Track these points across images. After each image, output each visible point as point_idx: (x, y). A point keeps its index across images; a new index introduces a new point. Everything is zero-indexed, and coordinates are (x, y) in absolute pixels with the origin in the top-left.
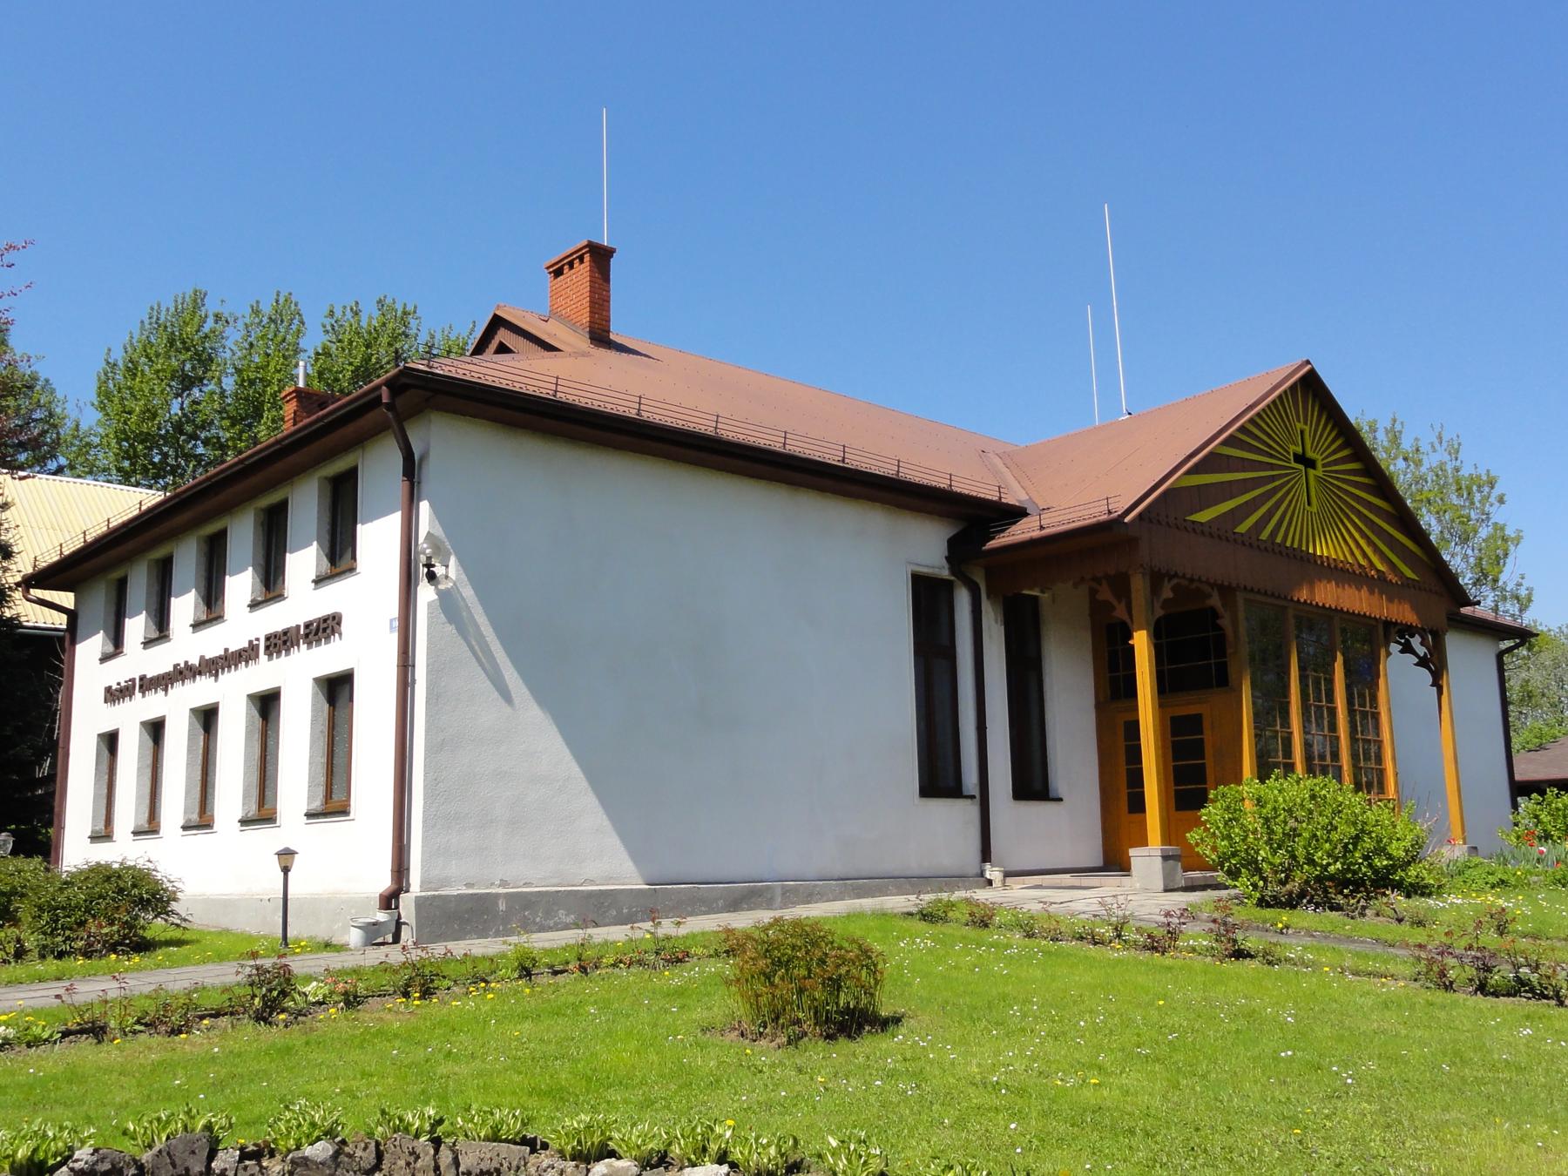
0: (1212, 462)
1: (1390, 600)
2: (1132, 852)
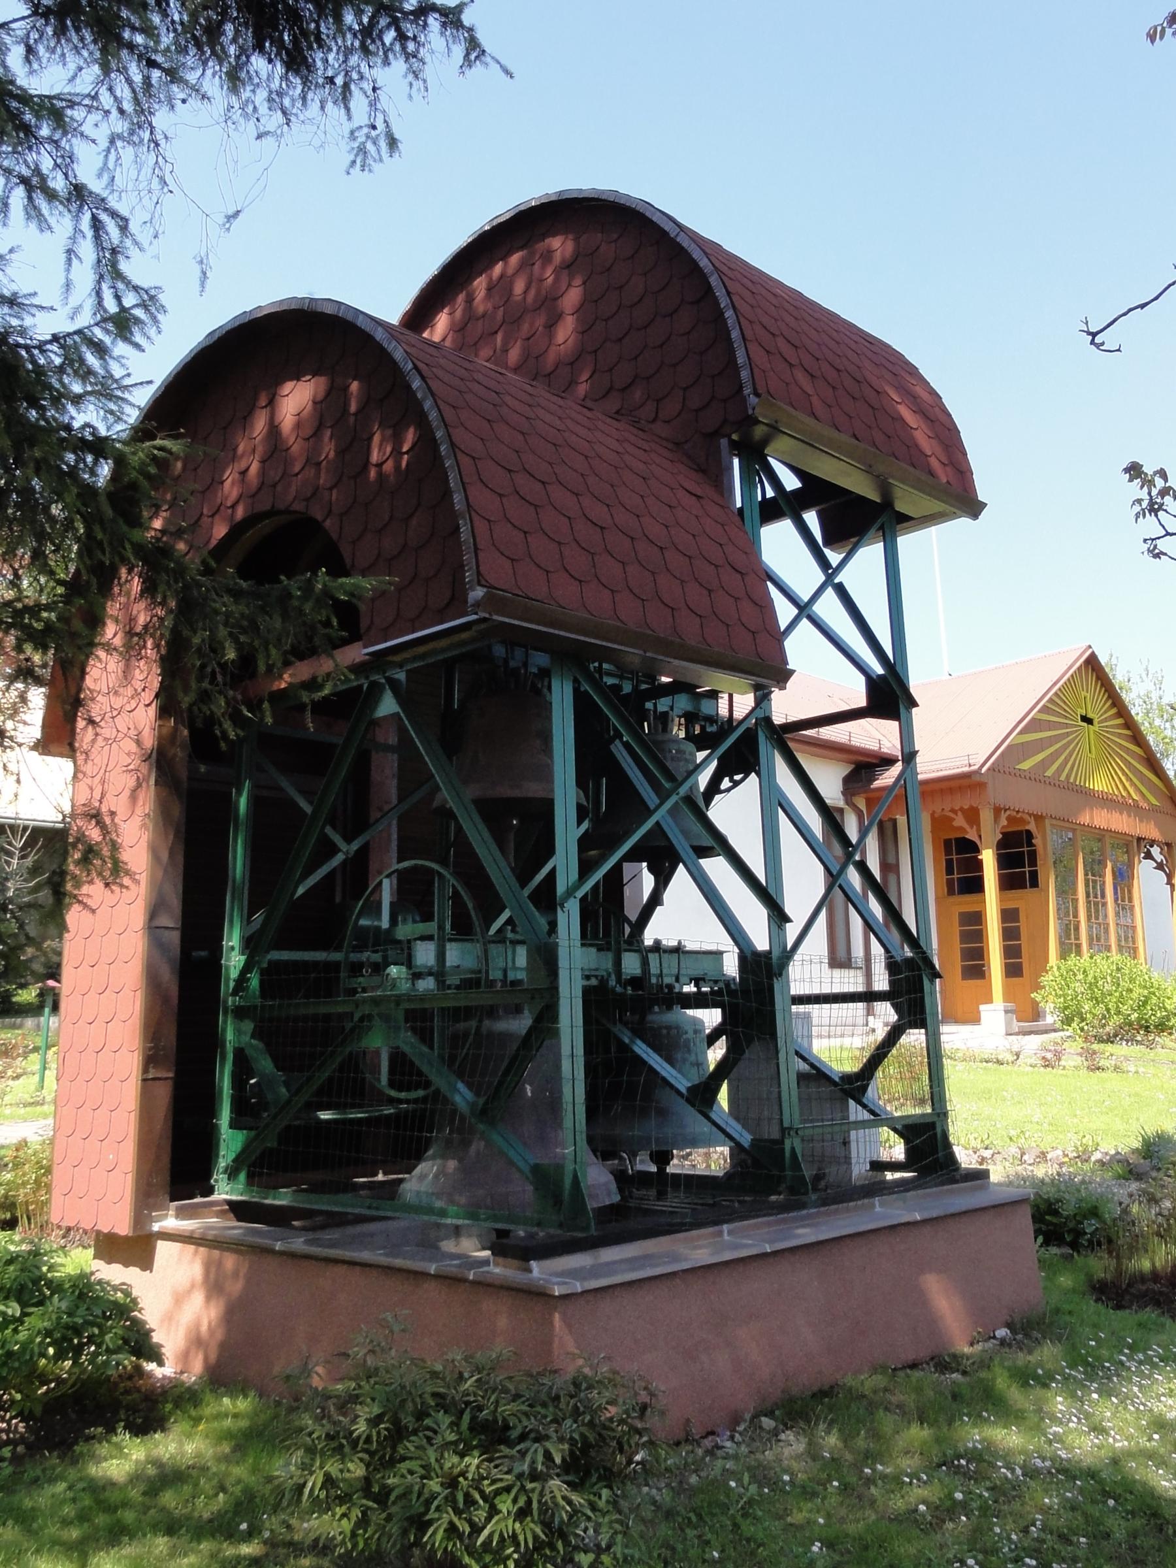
0: (1034, 725)
1: (1141, 821)
2: (982, 1007)
